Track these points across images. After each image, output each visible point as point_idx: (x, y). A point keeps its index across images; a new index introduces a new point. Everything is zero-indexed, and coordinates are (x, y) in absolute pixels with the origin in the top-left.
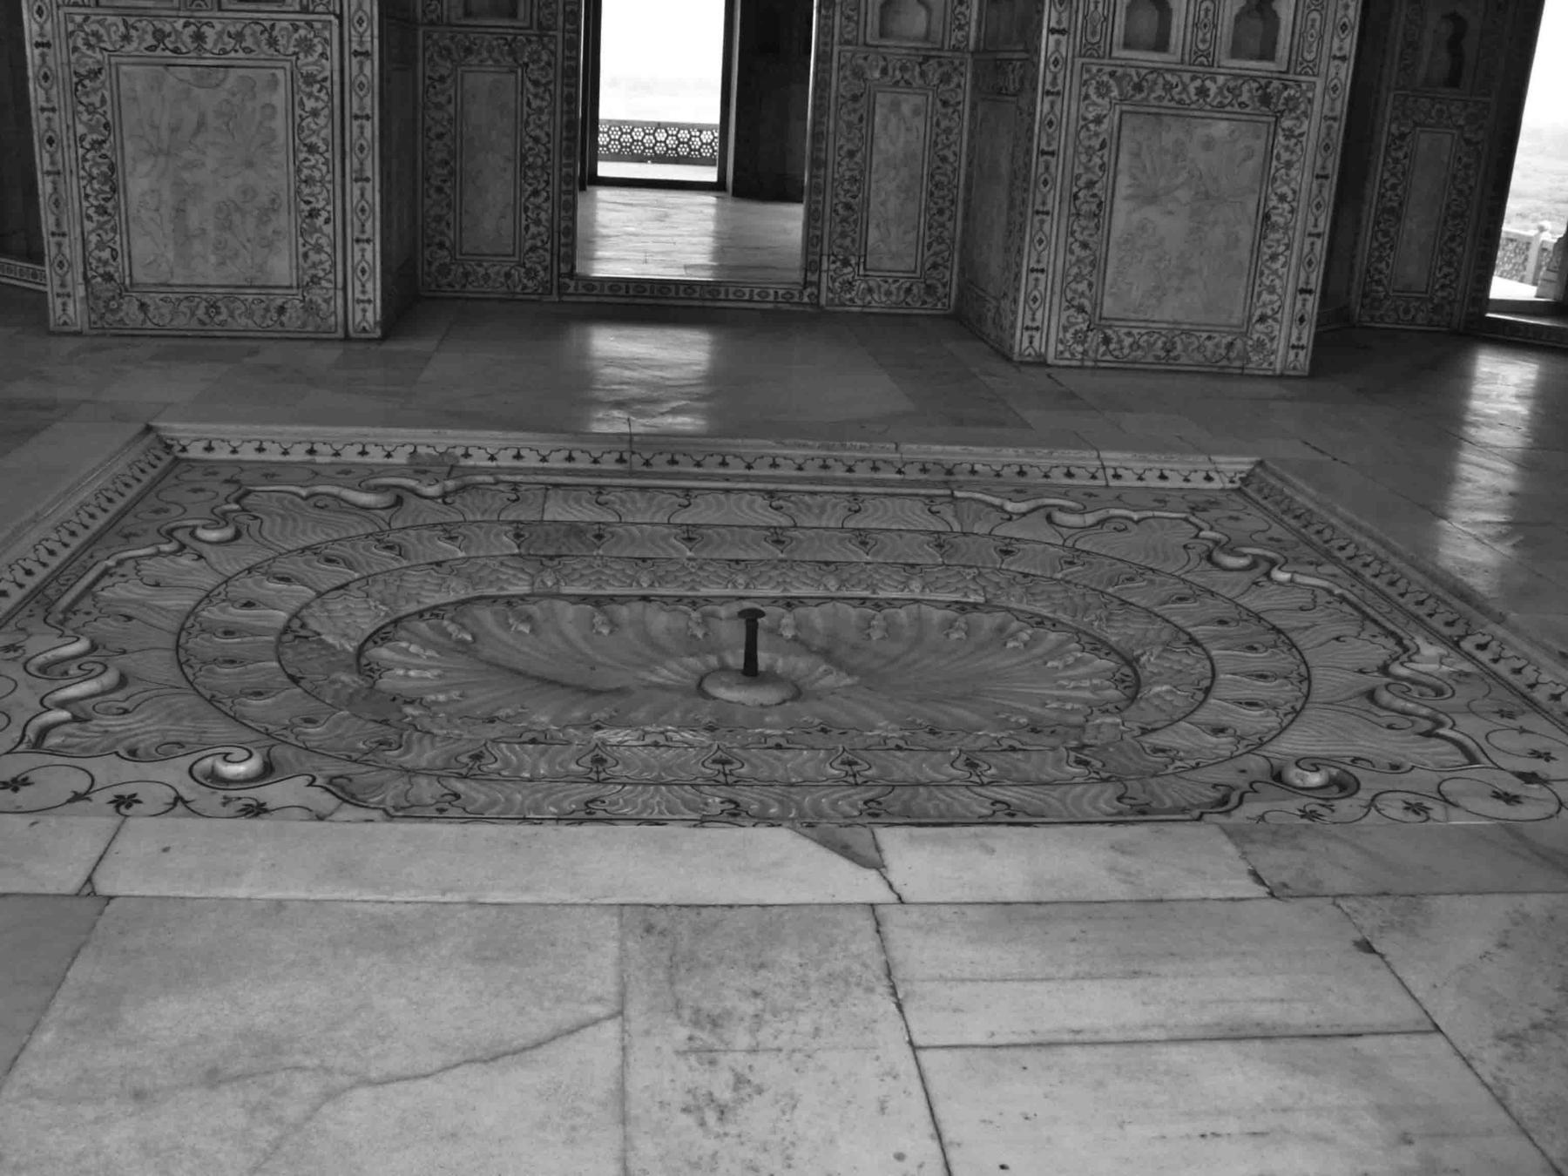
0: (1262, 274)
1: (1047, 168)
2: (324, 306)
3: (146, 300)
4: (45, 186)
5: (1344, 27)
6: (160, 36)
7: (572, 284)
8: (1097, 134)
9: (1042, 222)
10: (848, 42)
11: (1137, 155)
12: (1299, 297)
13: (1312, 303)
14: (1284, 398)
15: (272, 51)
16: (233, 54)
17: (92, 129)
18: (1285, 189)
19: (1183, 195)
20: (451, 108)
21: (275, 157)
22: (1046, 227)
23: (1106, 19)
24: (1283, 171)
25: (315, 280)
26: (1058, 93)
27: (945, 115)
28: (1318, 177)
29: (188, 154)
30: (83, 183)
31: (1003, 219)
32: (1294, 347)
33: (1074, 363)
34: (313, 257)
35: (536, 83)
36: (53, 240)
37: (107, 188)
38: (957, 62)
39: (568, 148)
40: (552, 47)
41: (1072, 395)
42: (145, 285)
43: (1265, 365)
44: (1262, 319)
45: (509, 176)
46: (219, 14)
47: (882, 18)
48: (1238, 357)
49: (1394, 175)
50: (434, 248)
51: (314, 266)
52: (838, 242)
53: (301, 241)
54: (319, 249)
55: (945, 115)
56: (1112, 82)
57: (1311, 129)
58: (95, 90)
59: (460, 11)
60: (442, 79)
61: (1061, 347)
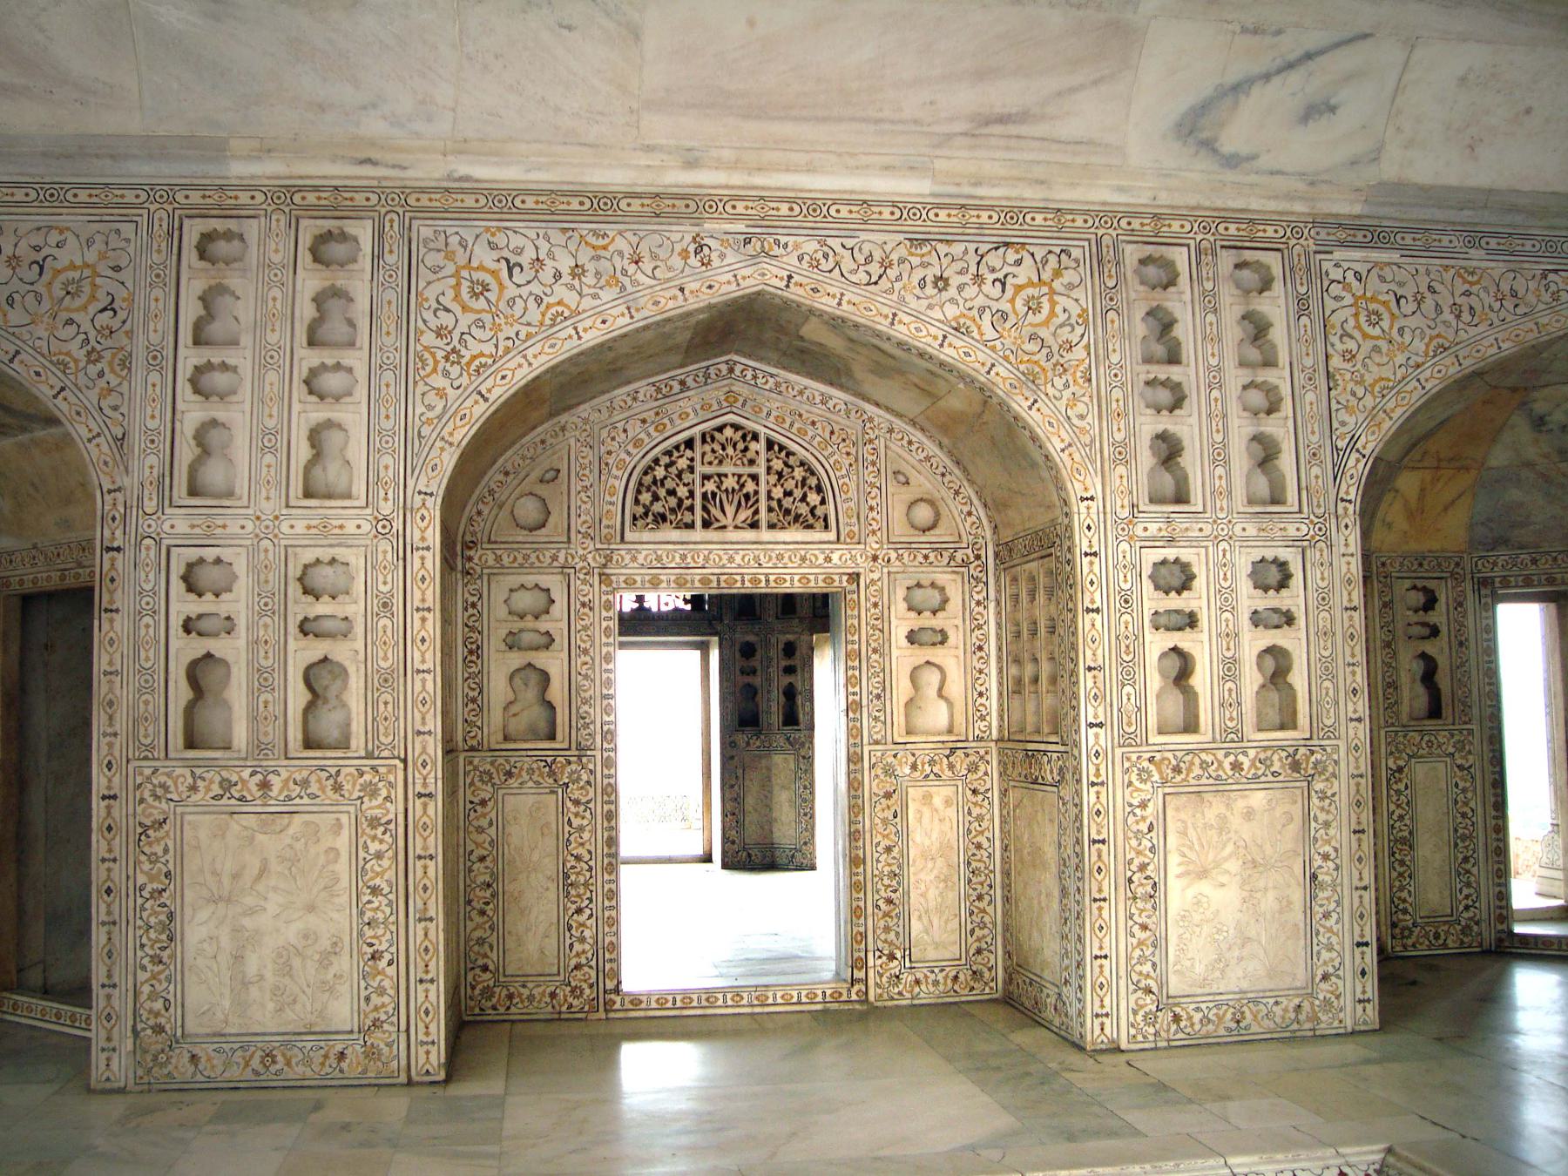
0: (1318, 934)
1: (1099, 856)
2: (386, 1050)
3: (196, 1051)
4: (98, 936)
5: (1355, 692)
6: (227, 785)
7: (618, 999)
8: (1144, 818)
9: (1100, 909)
10: (877, 743)
11: (1184, 833)
12: (1358, 951)
13: (1371, 954)
14: (1368, 1061)
15: (337, 796)
16: (297, 801)
17: (152, 879)
18: (1327, 848)
19: (1233, 866)
20: (492, 831)
21: (336, 900)
22: (1105, 913)
23: (1139, 709)
24: (1322, 832)
25: (377, 1024)
26: (1102, 784)
27: (975, 804)
28: (1355, 832)
29: (249, 901)
30: (140, 932)
31: (1055, 906)
32: (1360, 1001)
33: (1146, 1046)
34: (376, 1000)
35: (577, 803)
36: (102, 992)
37: (164, 937)
38: (982, 752)
39: (610, 864)
40: (591, 766)
41: (1162, 1087)
42: (197, 1035)
43: (1336, 1024)
44: (1325, 977)
45: (552, 895)
46: (286, 762)
47: (907, 716)
48: (1308, 1019)
49: (1398, 806)
50: (478, 971)
51: (376, 1009)
52: (883, 937)
53: (363, 984)
54: (381, 991)
55: (975, 804)
56: (1152, 767)
57: (1342, 788)
58: (158, 840)
59: (500, 737)
60: (483, 803)
61: (1133, 1032)
